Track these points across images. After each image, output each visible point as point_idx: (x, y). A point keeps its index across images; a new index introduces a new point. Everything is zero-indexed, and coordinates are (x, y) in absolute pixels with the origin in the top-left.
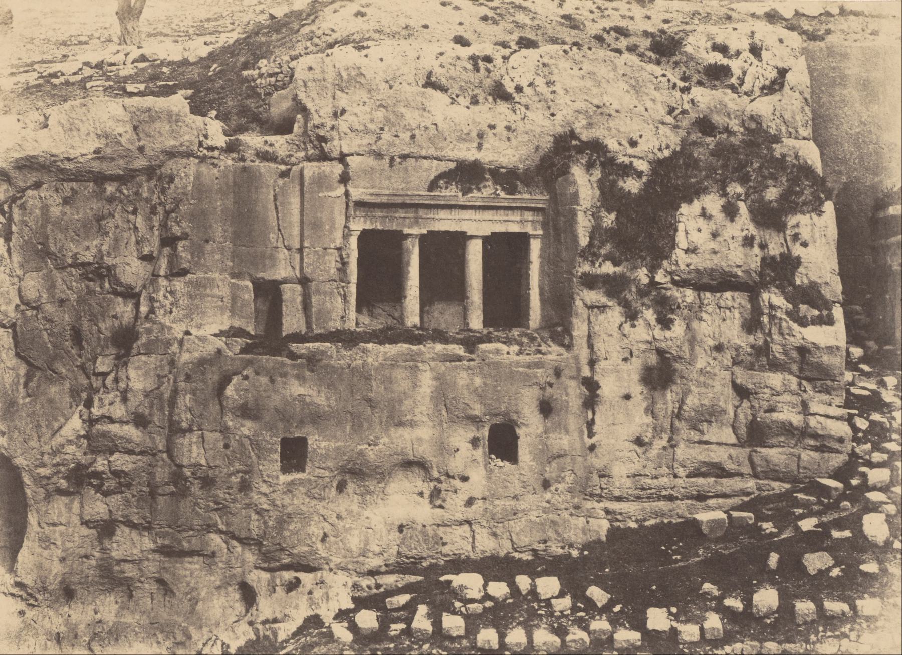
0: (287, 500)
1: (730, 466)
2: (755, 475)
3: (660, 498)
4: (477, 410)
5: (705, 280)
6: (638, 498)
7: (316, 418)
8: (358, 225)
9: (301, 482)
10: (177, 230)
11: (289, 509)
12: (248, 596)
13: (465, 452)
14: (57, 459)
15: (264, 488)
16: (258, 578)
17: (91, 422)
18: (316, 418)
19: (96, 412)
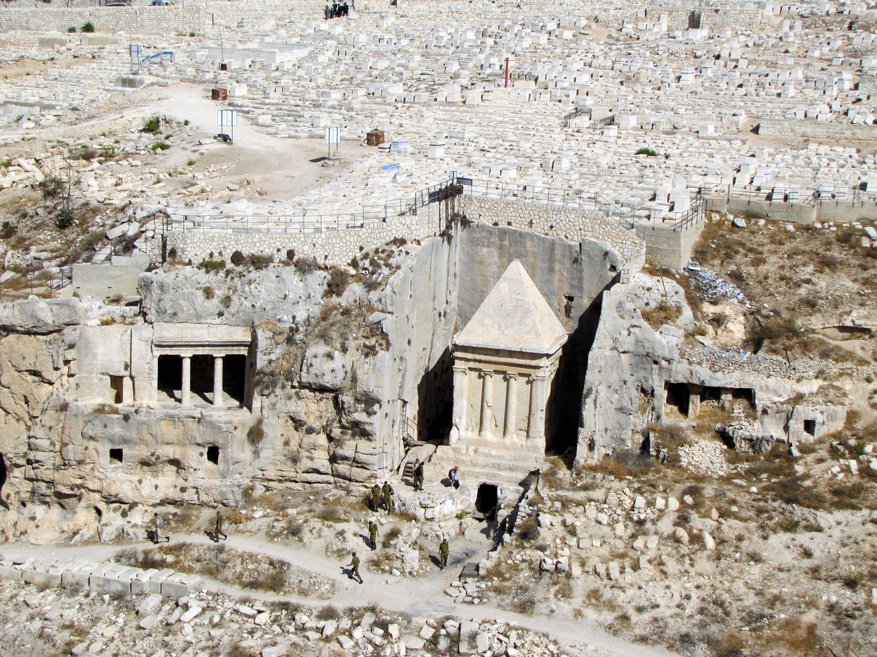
0: (113, 474)
1: (322, 470)
2: (333, 476)
3: (291, 481)
4: (200, 441)
5: (314, 387)
6: (280, 481)
7: (126, 441)
8: (158, 352)
9: (120, 467)
10: (69, 358)
11: (114, 479)
12: (99, 512)
13: (196, 458)
14: (16, 451)
15: (101, 470)
16: (102, 506)
17: (29, 437)
18: (126, 441)
19: (32, 434)
